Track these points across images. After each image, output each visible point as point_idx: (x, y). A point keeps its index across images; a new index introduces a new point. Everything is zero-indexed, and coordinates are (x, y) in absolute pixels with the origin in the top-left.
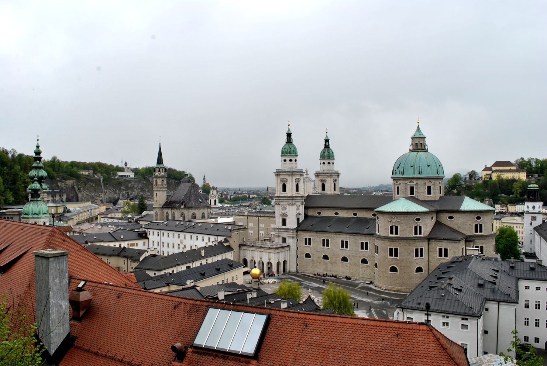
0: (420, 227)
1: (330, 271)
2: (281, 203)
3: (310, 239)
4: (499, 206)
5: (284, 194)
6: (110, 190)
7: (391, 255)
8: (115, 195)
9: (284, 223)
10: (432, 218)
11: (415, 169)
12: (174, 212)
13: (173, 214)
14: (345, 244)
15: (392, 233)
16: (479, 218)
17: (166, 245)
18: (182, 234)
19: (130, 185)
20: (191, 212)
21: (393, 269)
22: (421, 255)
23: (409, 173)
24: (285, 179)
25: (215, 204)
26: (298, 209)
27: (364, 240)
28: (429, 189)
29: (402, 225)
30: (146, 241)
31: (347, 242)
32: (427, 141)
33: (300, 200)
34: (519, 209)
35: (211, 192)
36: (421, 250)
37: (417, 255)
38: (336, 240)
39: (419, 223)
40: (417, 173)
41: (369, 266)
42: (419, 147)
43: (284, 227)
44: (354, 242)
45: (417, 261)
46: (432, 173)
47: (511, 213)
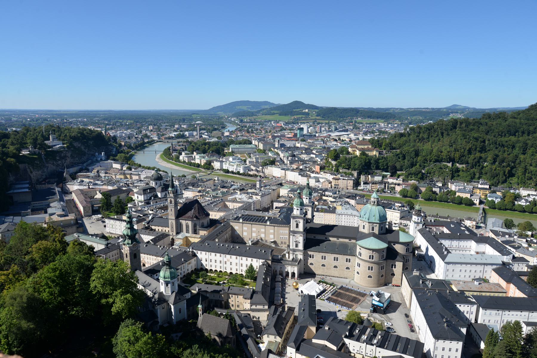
1: (326, 273)
5: (296, 230)
6: (50, 163)
7: (369, 269)
9: (297, 246)
14: (336, 259)
15: (370, 258)
16: (408, 245)
17: (213, 261)
18: (228, 256)
19: (62, 155)
20: (201, 221)
21: (370, 277)
27: (348, 257)
28: (382, 227)
30: (195, 258)
38: (330, 257)
42: (376, 203)
43: (296, 248)
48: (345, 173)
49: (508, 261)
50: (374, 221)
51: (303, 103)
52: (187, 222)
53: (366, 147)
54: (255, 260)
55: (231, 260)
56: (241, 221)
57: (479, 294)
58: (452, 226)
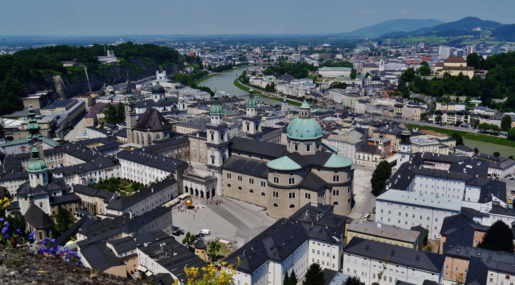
0: (293, 179)
3: (230, 174)
4: (440, 104)
5: (212, 142)
7: (274, 196)
8: (100, 82)
9: (213, 162)
13: (142, 134)
14: (252, 181)
15: (275, 182)
18: (143, 166)
20: (156, 133)
22: (294, 197)
25: (184, 108)
30: (119, 166)
31: (253, 180)
34: (457, 108)
36: (294, 194)
37: (290, 197)
38: (246, 178)
41: (266, 198)
43: (213, 165)
44: (258, 181)
45: (291, 201)
46: (310, 137)
47: (448, 112)
48: (415, 99)
49: (486, 212)
50: (296, 138)
51: (479, 19)
52: (142, 132)
53: (458, 65)
54: (163, 172)
55: (146, 171)
56: (198, 136)
57: (375, 238)
58: (460, 163)
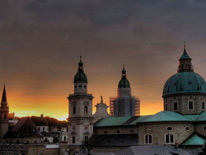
2: (72, 124)
5: (75, 116)
10: (187, 129)
11: (178, 86)
12: (12, 141)
23: (173, 91)
24: (75, 102)
26: (86, 128)
28: (191, 104)
29: (154, 134)
32: (193, 63)
33: (89, 121)
35: (62, 130)
39: (171, 132)
40: (179, 90)
43: (74, 144)
50: (175, 93)
